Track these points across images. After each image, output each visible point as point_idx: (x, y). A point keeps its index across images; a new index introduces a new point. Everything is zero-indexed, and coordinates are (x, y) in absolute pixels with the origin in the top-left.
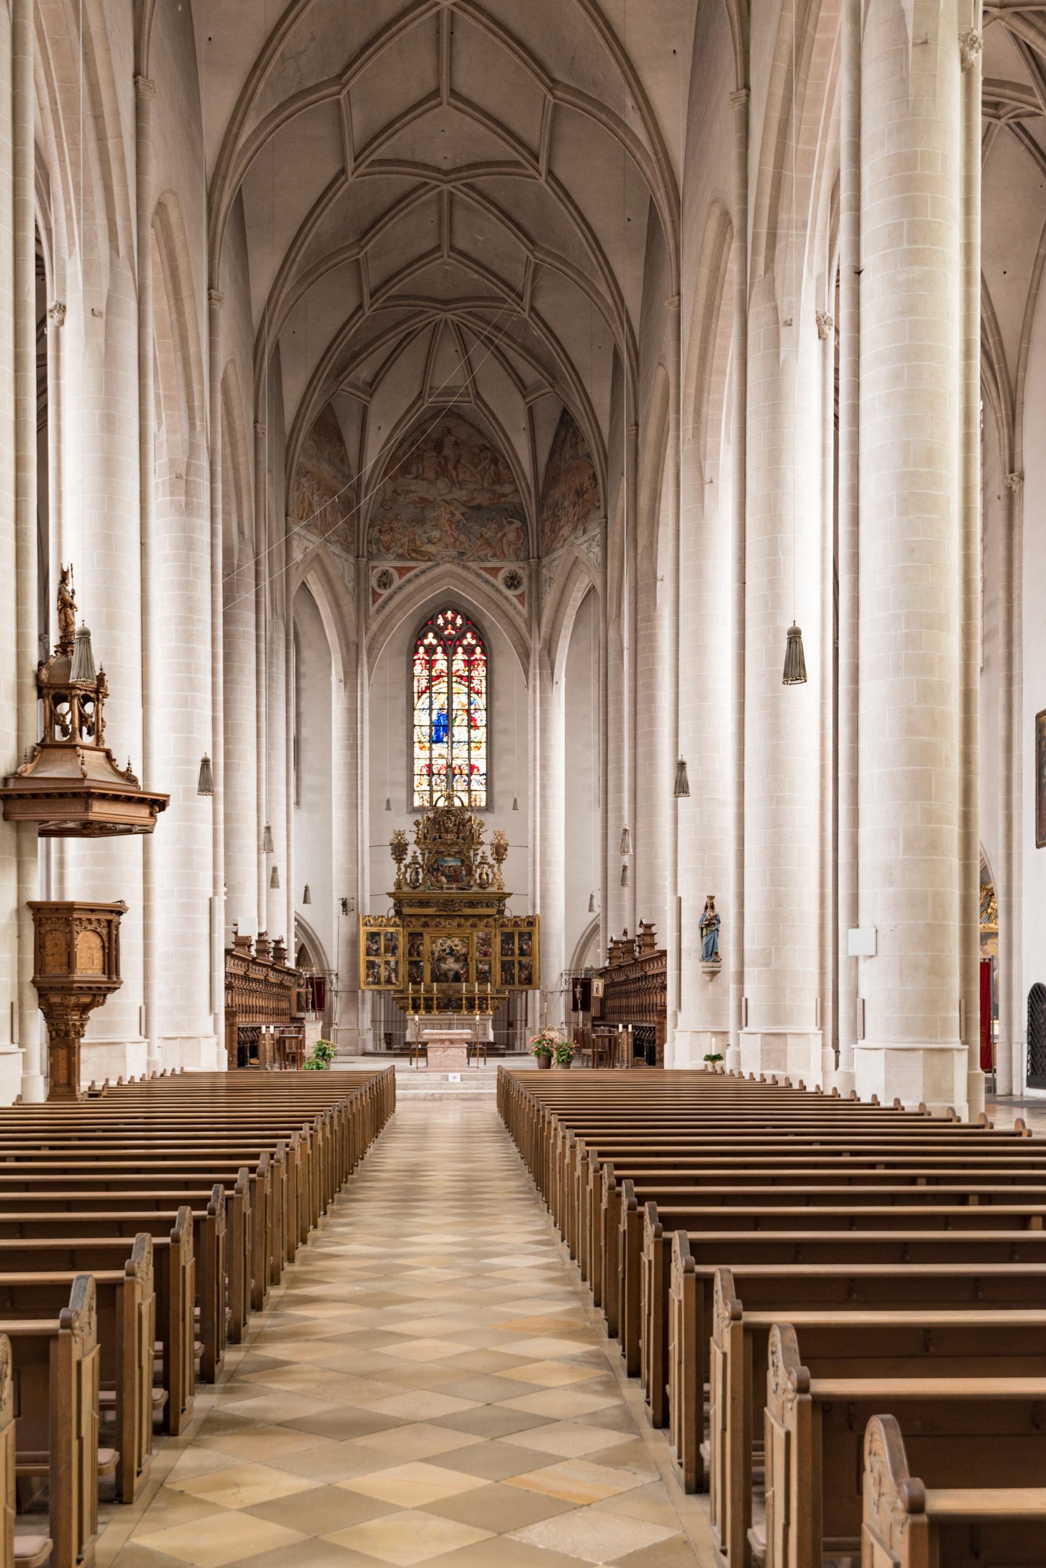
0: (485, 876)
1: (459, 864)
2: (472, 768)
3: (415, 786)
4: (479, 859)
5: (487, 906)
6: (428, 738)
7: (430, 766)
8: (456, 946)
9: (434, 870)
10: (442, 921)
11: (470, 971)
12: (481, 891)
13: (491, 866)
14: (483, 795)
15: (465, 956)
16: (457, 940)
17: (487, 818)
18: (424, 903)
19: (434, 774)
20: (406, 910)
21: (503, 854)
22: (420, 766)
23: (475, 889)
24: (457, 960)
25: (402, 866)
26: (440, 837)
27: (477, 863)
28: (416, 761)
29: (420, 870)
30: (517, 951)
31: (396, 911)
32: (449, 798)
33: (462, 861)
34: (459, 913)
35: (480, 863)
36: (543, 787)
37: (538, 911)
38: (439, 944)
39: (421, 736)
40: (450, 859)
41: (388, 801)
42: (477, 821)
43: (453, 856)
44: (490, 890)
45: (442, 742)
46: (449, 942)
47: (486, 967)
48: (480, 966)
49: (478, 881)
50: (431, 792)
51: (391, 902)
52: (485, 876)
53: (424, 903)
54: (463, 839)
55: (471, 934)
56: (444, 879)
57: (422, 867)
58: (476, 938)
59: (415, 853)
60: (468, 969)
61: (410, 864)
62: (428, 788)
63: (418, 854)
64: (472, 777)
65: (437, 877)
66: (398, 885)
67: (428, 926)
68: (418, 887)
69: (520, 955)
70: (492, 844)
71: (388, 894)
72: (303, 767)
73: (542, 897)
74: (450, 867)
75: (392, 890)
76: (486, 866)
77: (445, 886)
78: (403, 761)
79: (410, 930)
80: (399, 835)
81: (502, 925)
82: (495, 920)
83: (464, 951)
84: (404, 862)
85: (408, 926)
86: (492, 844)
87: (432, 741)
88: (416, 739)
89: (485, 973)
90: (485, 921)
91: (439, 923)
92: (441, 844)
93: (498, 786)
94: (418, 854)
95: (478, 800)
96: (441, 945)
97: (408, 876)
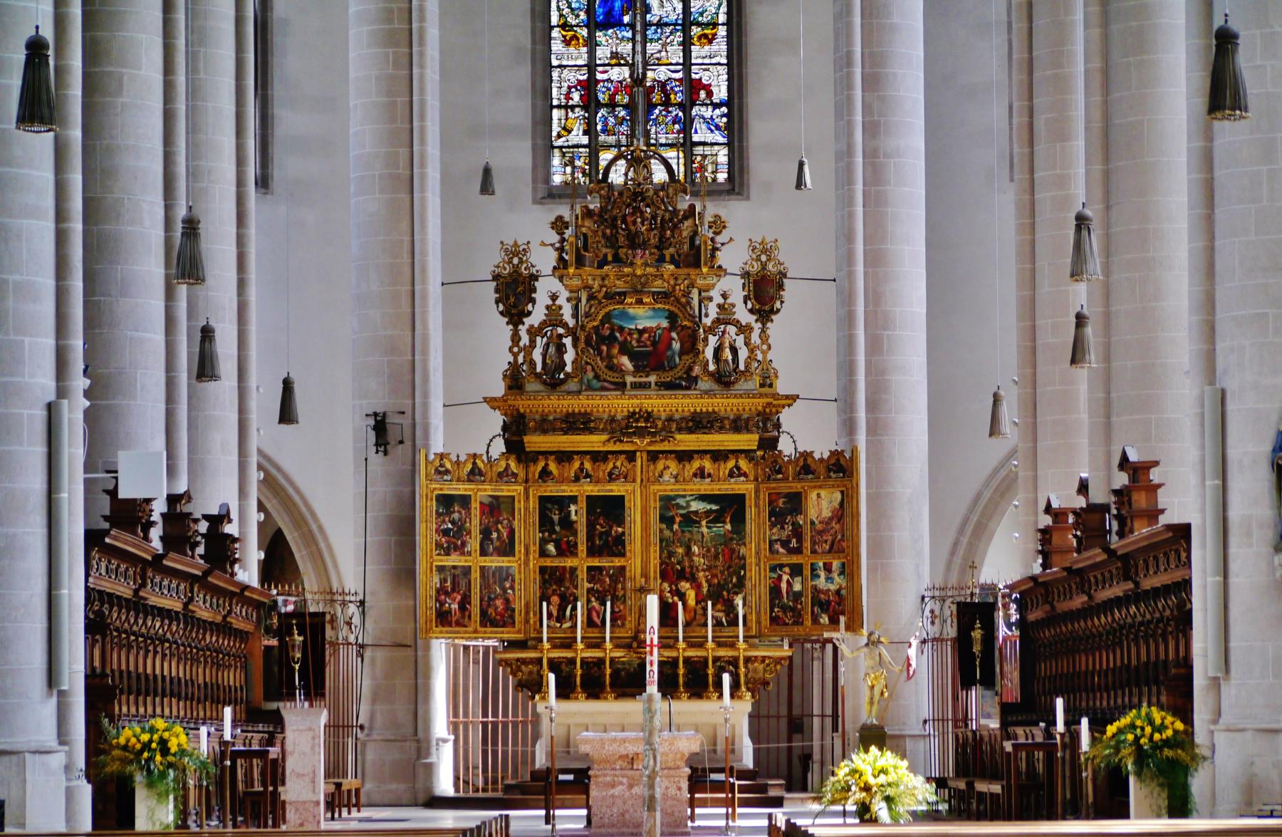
0: (727, 354)
1: (665, 324)
2: (694, 88)
3: (554, 134)
4: (713, 311)
6: (583, 16)
7: (589, 87)
9: (602, 339)
12: (715, 386)
13: (744, 330)
14: (723, 158)
17: (732, 211)
18: (578, 423)
19: (599, 105)
20: (534, 441)
21: (773, 299)
22: (565, 85)
23: (705, 384)
25: (523, 330)
27: (708, 321)
28: (555, 74)
29: (568, 341)
31: (507, 443)
32: (638, 162)
33: (672, 317)
34: (665, 446)
35: (718, 321)
36: (871, 129)
39: (566, 11)
41: (487, 172)
42: (708, 218)
45: (620, 24)
49: (712, 367)
50: (594, 149)
51: (496, 420)
52: (727, 354)
53: (578, 423)
54: (673, 261)
56: (625, 361)
57: (572, 332)
59: (554, 297)
61: (544, 324)
62: (585, 140)
64: (694, 113)
65: (610, 357)
66: (514, 380)
68: (563, 382)
70: (746, 275)
72: (278, 90)
73: (872, 405)
74: (641, 332)
76: (732, 330)
77: (629, 379)
78: (523, 74)
80: (516, 254)
84: (528, 321)
86: (746, 275)
87: (594, 25)
88: (555, 20)
93: (759, 131)
94: (561, 301)
95: (710, 168)
97: (537, 356)
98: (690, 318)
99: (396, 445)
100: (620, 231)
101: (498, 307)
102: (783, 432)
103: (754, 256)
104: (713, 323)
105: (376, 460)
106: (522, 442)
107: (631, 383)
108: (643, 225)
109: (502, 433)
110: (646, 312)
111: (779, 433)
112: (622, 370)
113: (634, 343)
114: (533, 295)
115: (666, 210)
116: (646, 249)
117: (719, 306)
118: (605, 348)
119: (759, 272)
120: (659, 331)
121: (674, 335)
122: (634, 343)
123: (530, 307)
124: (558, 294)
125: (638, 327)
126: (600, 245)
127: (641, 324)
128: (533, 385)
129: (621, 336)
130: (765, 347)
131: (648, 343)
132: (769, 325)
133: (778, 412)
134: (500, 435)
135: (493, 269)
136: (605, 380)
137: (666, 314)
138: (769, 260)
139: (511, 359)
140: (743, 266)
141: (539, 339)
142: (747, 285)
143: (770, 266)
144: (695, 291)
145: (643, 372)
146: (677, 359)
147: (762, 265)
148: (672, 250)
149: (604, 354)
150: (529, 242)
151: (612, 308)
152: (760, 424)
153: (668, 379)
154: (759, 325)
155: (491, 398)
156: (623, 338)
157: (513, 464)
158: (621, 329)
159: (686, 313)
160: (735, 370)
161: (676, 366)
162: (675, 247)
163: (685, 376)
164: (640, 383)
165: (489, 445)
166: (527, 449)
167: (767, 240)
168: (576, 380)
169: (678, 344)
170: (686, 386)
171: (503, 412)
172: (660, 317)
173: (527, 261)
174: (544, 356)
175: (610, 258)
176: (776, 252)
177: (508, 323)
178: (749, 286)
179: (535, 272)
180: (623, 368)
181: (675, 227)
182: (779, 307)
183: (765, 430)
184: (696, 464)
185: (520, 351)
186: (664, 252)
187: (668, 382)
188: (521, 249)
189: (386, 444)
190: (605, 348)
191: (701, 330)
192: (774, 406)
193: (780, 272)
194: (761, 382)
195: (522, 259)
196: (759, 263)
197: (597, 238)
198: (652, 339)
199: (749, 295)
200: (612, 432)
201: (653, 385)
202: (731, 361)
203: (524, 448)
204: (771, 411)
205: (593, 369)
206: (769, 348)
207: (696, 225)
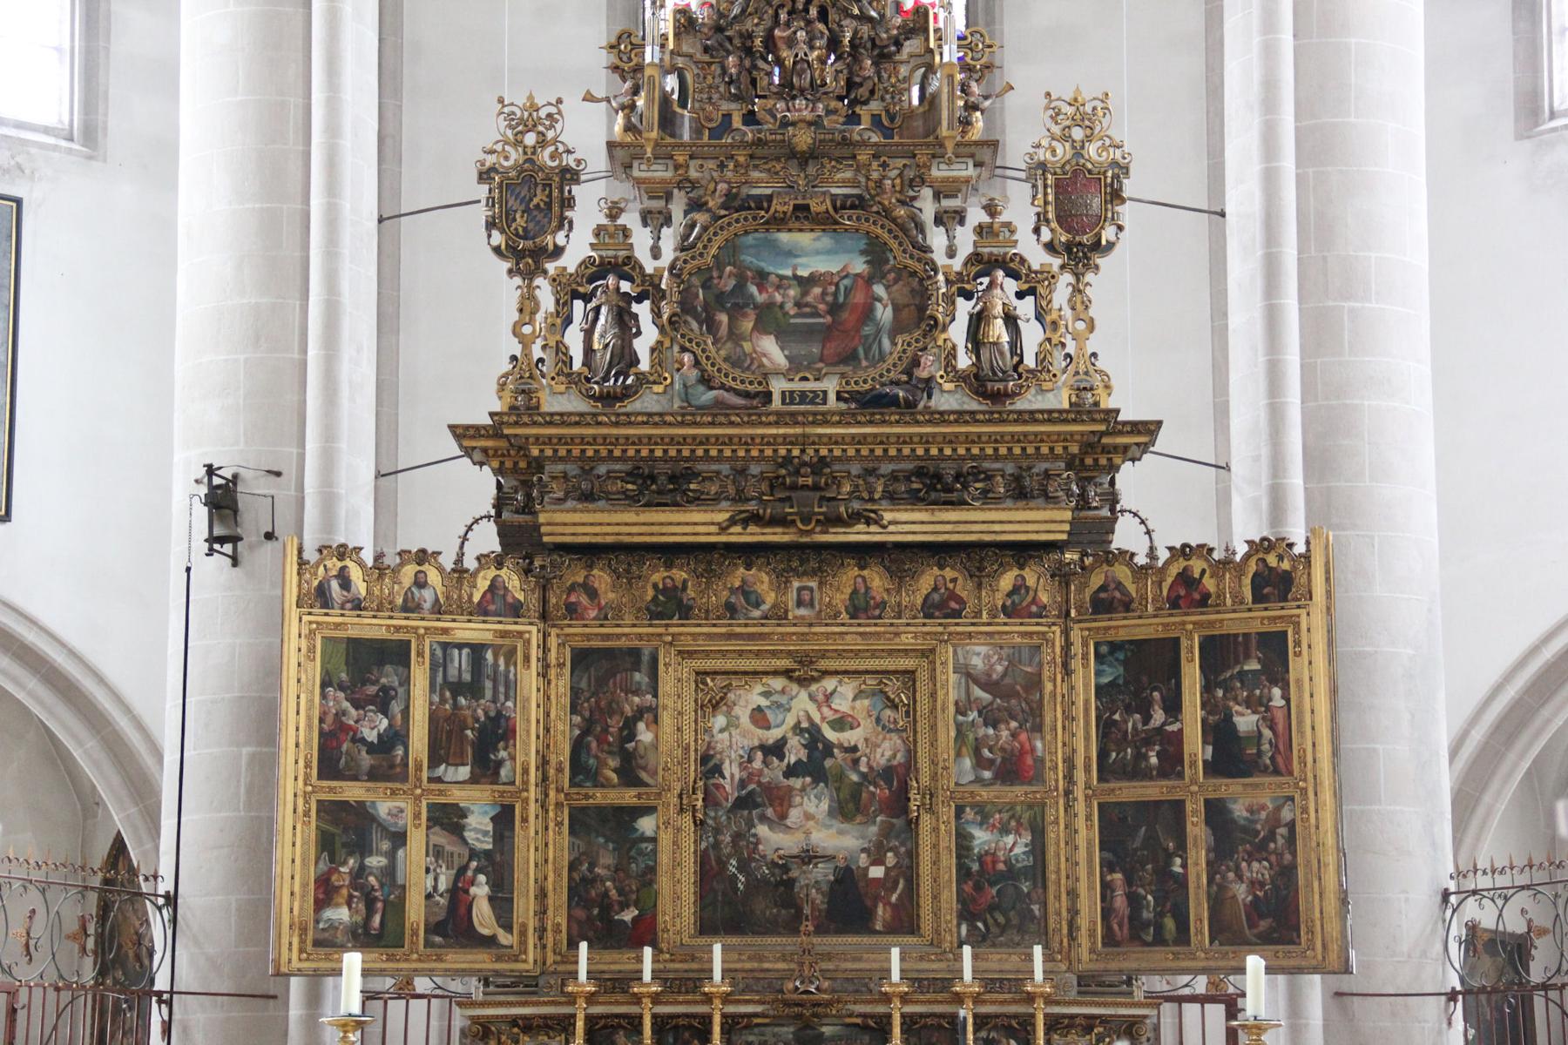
1: (859, 266)
4: (965, 240)
5: (1020, 493)
8: (841, 723)
10: (762, 580)
11: (925, 867)
12: (973, 405)
15: (898, 778)
16: (848, 689)
21: (1099, 221)
23: (948, 398)
24: (848, 808)
26: (750, 118)
27: (957, 264)
30: (1196, 747)
31: (504, 533)
33: (876, 253)
34: (859, 534)
37: (1297, 534)
38: (743, 714)
40: (804, 239)
43: (825, 223)
44: (1030, 401)
46: (802, 704)
47: (1017, 845)
48: (982, 838)
49: (964, 361)
52: (998, 330)
55: (928, 654)
56: (771, 350)
58: (953, 678)
60: (913, 855)
63: (630, 219)
65: (735, 336)
67: (685, 612)
68: (626, 394)
69: (1212, 768)
71: (461, 433)
73: (1318, 462)
74: (806, 283)
75: (482, 406)
76: (1011, 286)
77: (778, 386)
79: (588, 631)
80: (529, 125)
81: (1107, 603)
82: (1062, 576)
83: (887, 751)
84: (551, 267)
85: (572, 611)
89: (1012, 873)
90: (1007, 581)
91: (745, 591)
92: (760, 152)
94: (630, 219)
96: (759, 717)
97: (574, 340)
99: (260, 544)
101: (489, 236)
102: (1122, 511)
103: (1056, 130)
104: (965, 264)
105: (213, 569)
106: (537, 527)
107: (783, 392)
108: (812, 48)
109: (493, 512)
110: (817, 239)
111: (1112, 510)
112: (761, 365)
113: (790, 308)
114: (568, 214)
115: (864, 18)
116: (819, 100)
117: (980, 230)
118: (723, 318)
119: (1068, 162)
120: (846, 282)
121: (879, 290)
122: (790, 308)
123: (560, 239)
124: (622, 205)
125: (800, 273)
126: (715, 97)
127: (805, 266)
128: (563, 399)
129: (760, 292)
130: (1081, 325)
131: (822, 307)
132: (1089, 277)
133: (1113, 468)
134: (489, 517)
135: (482, 156)
136: (723, 387)
137: (862, 244)
138: (1089, 138)
139: (517, 350)
140: (1032, 150)
141: (578, 305)
142: (1041, 189)
143: (1092, 150)
144: (927, 193)
145: (808, 368)
146: (886, 343)
147: (1074, 147)
148: (875, 106)
149: (723, 331)
150: (559, 101)
152: (1074, 487)
153: (867, 387)
154: (1068, 278)
155: (467, 427)
157: (513, 581)
158: (761, 277)
159: (907, 242)
160: (1015, 368)
161: (882, 358)
162: (883, 99)
163: (904, 378)
164: (803, 394)
165: (465, 539)
166: (546, 539)
167: (1086, 94)
168: (658, 389)
169: (889, 309)
170: (906, 400)
171: (496, 464)
173: (555, 141)
174: (588, 334)
175: (737, 122)
176: (1105, 122)
177: (510, 271)
178: (1046, 194)
179: (573, 165)
180: (765, 360)
181: (883, 57)
182: (1112, 238)
183: (1083, 503)
184: (927, 580)
185: (534, 336)
186: (857, 110)
187: (867, 392)
188: (543, 113)
189: (235, 539)
190: (723, 318)
191: (941, 277)
192: (1106, 450)
193: (1115, 164)
194: (1074, 399)
195: (544, 135)
196: (1068, 145)
198: (829, 299)
199: (1046, 212)
200: (740, 498)
201: (832, 397)
202: (1007, 347)
203: (541, 536)
204: (1096, 460)
205: (697, 363)
206: (1091, 326)
207: (931, 51)
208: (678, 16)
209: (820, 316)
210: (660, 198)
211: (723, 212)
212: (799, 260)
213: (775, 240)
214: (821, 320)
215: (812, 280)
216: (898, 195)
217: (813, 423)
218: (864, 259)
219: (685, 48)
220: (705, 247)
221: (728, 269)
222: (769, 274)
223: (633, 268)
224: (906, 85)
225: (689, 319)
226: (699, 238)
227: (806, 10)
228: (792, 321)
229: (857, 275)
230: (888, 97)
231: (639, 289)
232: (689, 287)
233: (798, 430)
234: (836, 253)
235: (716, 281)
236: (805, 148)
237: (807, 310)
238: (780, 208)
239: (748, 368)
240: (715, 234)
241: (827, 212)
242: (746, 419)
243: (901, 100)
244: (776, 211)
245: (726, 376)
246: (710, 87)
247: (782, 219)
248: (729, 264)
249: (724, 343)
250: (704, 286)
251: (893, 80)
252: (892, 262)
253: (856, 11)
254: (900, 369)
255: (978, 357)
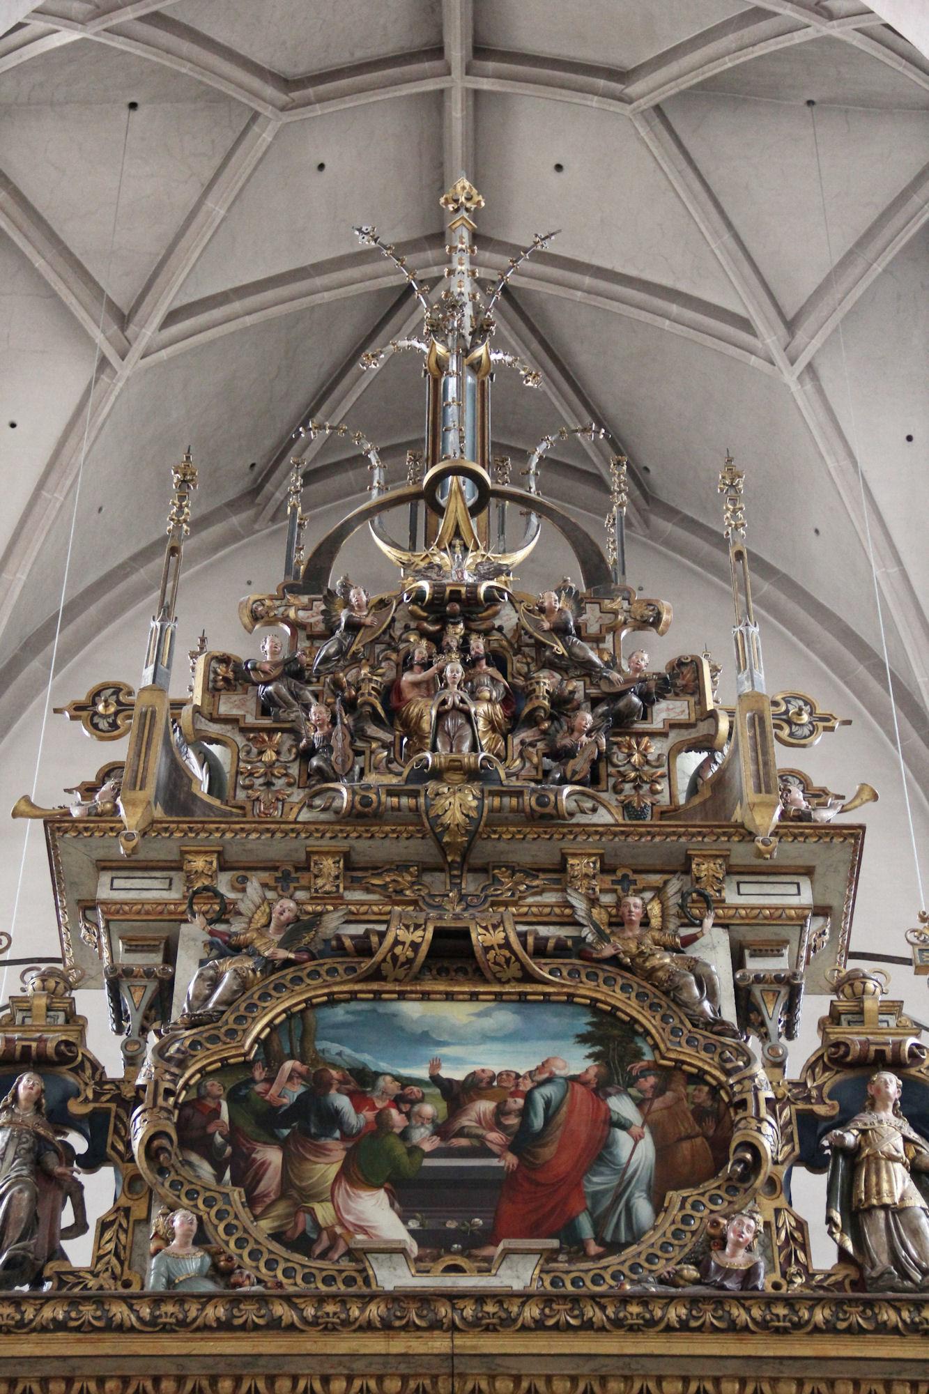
40: (458, 1014)
98: (701, 1035)
100: (372, 730)
108: (475, 696)
113: (423, 1137)
118: (273, 1157)
122: (423, 1137)
125: (445, 1073)
126: (280, 783)
127: (458, 1061)
129: (358, 1109)
131: (495, 1138)
137: (583, 1023)
145: (466, 1253)
146: (643, 1209)
149: (270, 1182)
151: (318, 992)
156: (369, 1115)
161: (636, 1236)
163: (691, 1272)
172: (556, 1036)
190: (273, 1157)
197: (269, 756)
198: (513, 1121)
208: (214, 664)
209: (490, 1154)
210: (151, 949)
211: (283, 954)
212: (444, 1051)
213: (394, 1015)
214: (494, 1162)
215: (475, 1086)
216: (657, 935)
217: (480, 1325)
218: (587, 1050)
219: (224, 709)
220: (240, 1019)
221: (289, 1065)
222: (377, 1075)
223: (81, 1066)
224: (664, 770)
225: (194, 1158)
226: (228, 1002)
227: (464, 648)
228: (427, 1162)
229: (573, 1079)
230: (628, 786)
231: (91, 1106)
232: (200, 1098)
233: (439, 1344)
234: (525, 1039)
235: (259, 1088)
236: (459, 817)
237: (464, 1142)
238: (403, 935)
239: (323, 1256)
240: (265, 996)
241: (507, 945)
242: (310, 1312)
243: (654, 792)
244: (397, 942)
245: (271, 1264)
246: (271, 765)
247: (410, 961)
248: (291, 1057)
249: (273, 1203)
250: (232, 1098)
251: (636, 758)
252: (648, 1056)
253: (560, 649)
254: (676, 1254)
255: (859, 1241)
